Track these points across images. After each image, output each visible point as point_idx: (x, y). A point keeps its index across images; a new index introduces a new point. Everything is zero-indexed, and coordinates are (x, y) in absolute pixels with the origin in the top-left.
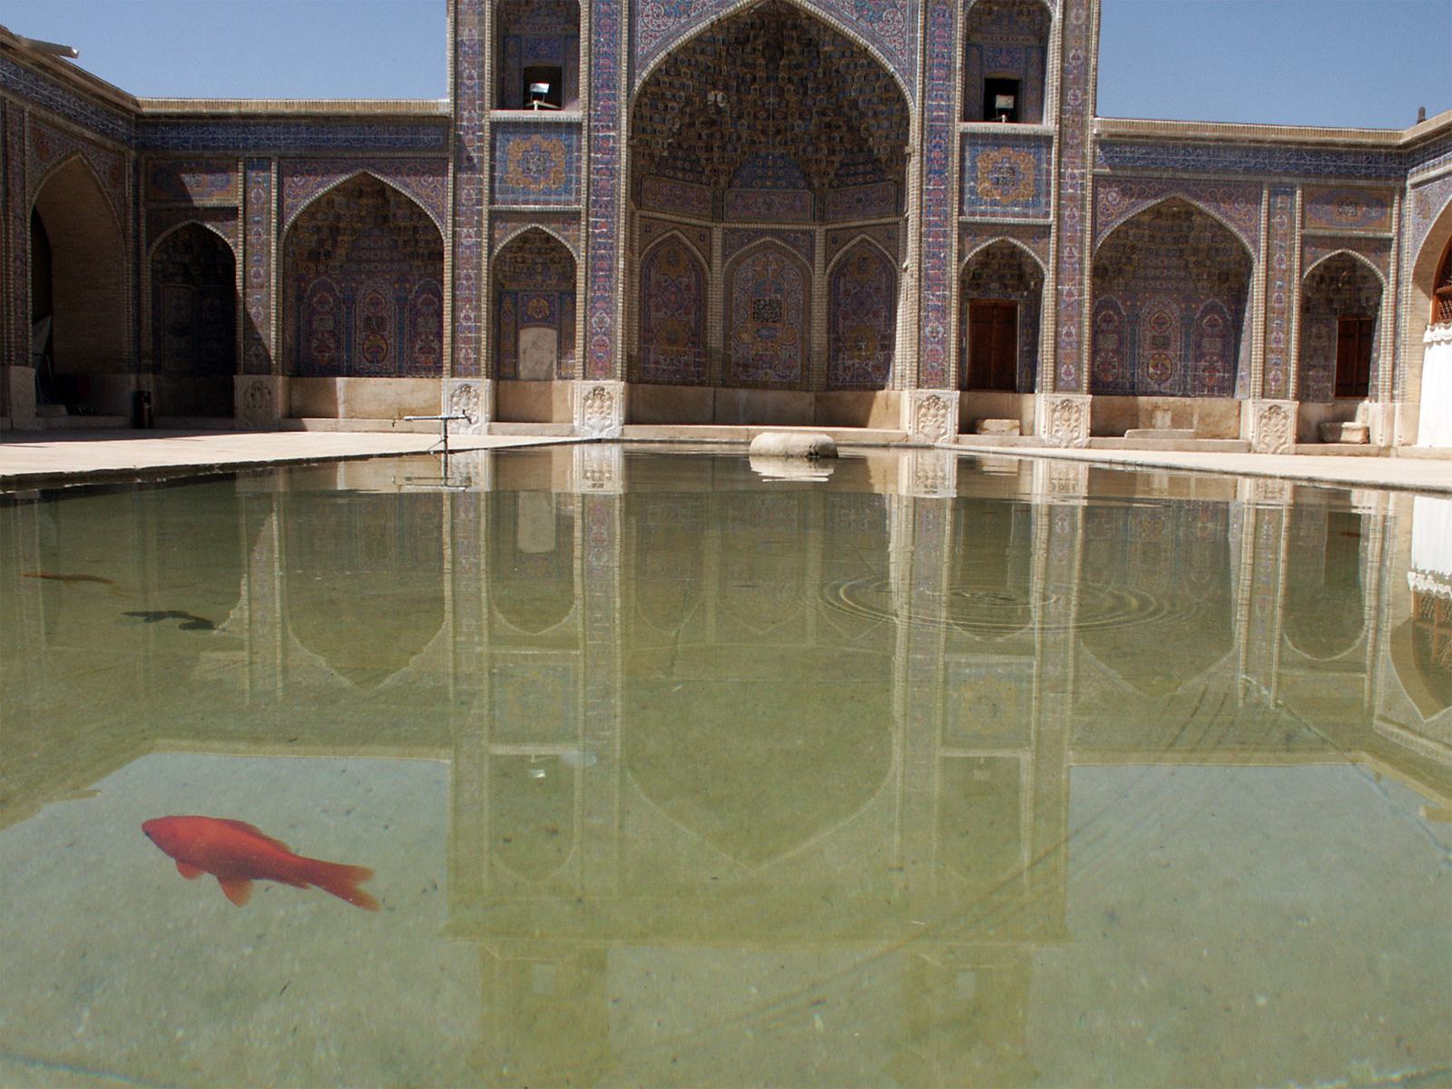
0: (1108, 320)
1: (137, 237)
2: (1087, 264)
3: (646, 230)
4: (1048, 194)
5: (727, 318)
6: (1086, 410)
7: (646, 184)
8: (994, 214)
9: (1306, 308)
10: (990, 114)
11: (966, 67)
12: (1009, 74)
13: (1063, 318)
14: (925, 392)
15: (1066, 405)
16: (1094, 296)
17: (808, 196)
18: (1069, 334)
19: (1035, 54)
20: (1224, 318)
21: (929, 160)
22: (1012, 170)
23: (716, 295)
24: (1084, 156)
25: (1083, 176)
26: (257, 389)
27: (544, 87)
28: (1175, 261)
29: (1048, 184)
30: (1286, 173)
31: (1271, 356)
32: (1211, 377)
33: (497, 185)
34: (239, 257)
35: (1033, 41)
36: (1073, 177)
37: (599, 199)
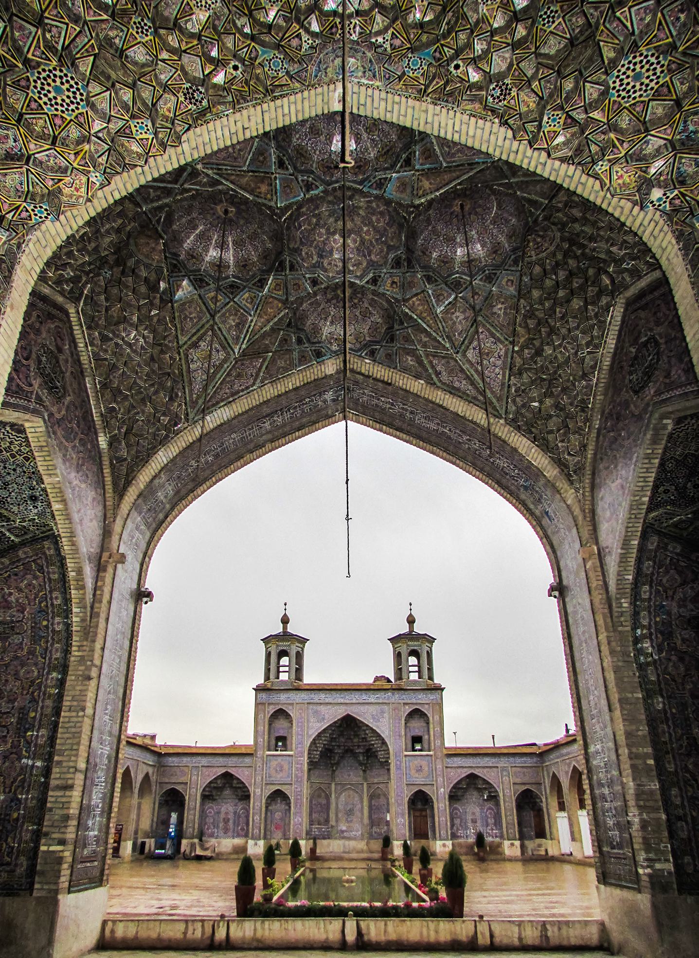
0: (456, 814)
2: (447, 797)
3: (311, 787)
5: (337, 816)
9: (520, 807)
10: (414, 750)
11: (406, 735)
12: (419, 734)
16: (450, 805)
17: (361, 773)
19: (426, 729)
27: (280, 744)
28: (475, 793)
34: (187, 798)
35: (425, 725)
37: (299, 781)
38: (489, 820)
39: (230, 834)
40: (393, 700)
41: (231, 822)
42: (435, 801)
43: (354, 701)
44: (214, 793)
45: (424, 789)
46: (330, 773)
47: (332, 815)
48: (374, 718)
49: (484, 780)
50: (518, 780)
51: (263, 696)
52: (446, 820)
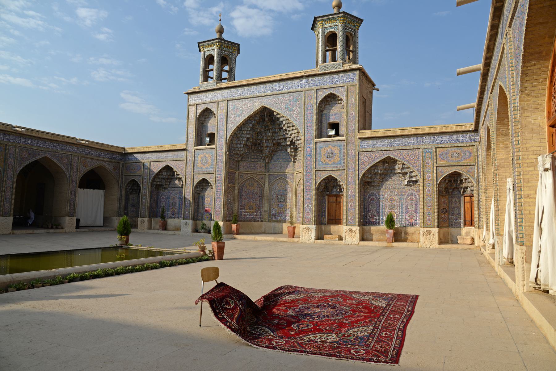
1: (122, 183)
4: (344, 159)
5: (270, 201)
6: (357, 232)
7: (241, 164)
8: (326, 167)
13: (349, 201)
14: (305, 226)
15: (351, 231)
18: (351, 206)
20: (416, 198)
21: (306, 152)
22: (332, 153)
23: (266, 194)
24: (355, 146)
25: (355, 152)
26: (143, 221)
29: (344, 156)
30: (429, 144)
31: (426, 211)
32: (411, 219)
33: (195, 167)
36: (352, 153)
38: (409, 207)
39: (176, 215)
40: (306, 88)
41: (177, 205)
42: (344, 186)
43: (269, 93)
44: (164, 183)
45: (334, 175)
46: (264, 164)
47: (265, 202)
48: (286, 108)
49: (403, 164)
50: (445, 162)
51: (193, 99)
52: (355, 206)
